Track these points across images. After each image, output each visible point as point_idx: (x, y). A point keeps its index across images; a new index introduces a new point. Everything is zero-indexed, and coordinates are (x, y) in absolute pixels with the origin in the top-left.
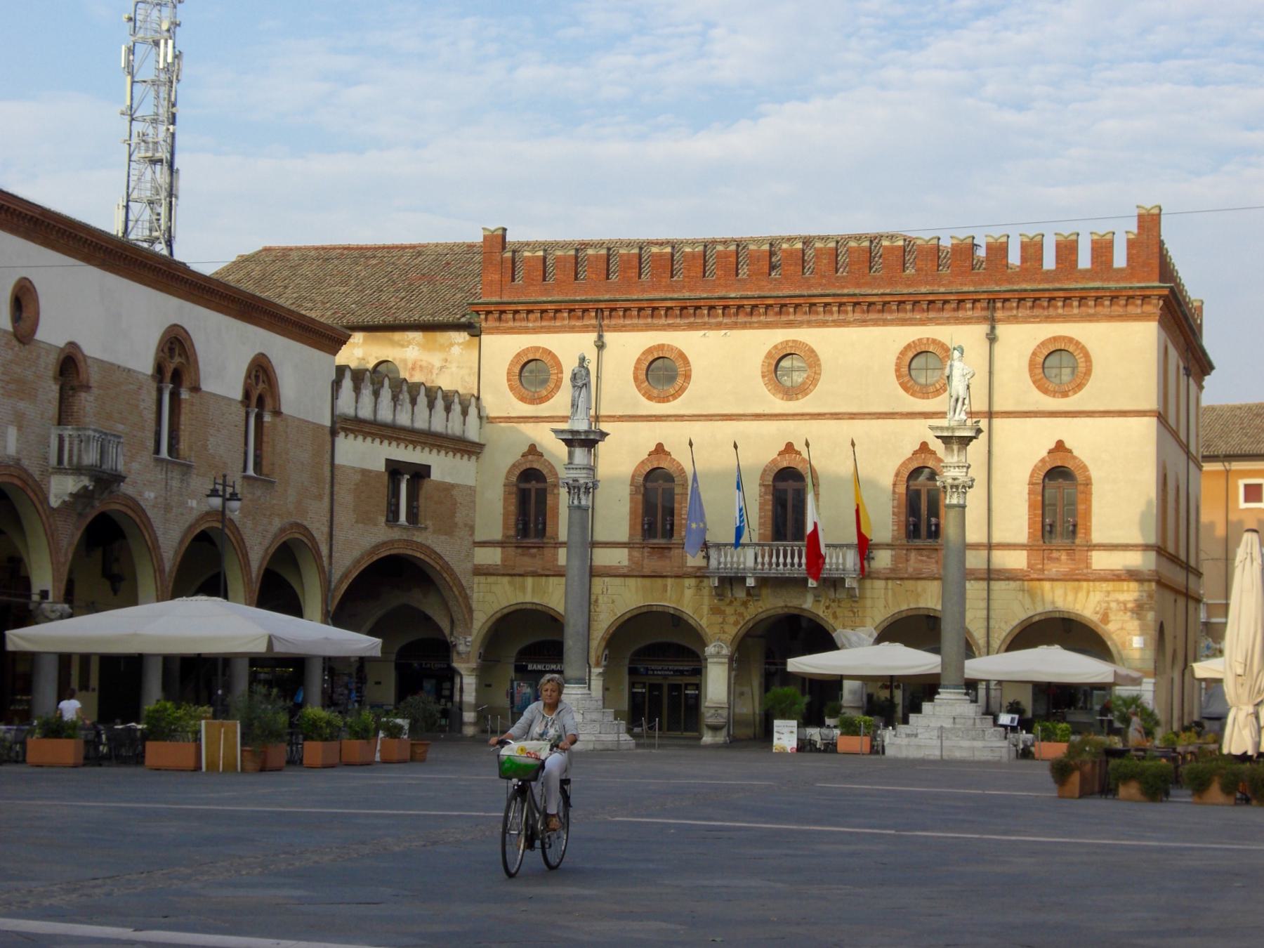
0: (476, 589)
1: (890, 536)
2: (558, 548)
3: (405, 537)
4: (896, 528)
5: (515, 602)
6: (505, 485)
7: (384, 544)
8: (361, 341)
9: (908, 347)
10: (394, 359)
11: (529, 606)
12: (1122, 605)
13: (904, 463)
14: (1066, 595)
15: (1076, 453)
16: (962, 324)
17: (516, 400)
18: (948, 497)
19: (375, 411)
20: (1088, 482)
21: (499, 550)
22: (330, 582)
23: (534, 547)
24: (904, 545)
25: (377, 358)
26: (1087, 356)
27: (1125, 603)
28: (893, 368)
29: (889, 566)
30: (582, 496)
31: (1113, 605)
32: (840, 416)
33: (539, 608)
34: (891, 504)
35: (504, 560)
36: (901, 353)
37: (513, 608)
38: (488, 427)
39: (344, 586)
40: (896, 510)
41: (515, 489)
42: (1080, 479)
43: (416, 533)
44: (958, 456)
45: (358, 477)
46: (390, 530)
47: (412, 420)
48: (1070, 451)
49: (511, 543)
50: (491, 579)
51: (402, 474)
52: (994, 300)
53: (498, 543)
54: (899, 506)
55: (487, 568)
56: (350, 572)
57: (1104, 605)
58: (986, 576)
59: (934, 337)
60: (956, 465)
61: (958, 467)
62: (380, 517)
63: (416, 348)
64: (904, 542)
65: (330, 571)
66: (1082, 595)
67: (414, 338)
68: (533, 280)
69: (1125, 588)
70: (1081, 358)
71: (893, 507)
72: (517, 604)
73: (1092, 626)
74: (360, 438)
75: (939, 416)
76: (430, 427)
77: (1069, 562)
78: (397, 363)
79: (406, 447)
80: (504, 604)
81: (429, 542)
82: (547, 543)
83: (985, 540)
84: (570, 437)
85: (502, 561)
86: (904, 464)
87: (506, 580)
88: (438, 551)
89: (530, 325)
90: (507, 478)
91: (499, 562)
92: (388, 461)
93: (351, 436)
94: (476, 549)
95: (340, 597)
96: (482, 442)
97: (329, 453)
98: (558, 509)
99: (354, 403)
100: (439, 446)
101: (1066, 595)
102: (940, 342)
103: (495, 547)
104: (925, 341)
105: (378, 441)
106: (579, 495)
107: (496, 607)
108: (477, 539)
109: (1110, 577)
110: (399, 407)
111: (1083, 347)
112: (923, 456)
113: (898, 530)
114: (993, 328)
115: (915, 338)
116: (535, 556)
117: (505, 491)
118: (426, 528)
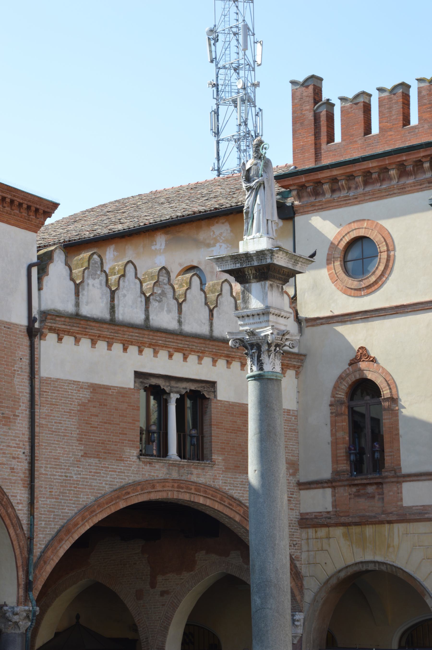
0: (305, 548)
2: (400, 483)
3: (175, 475)
5: (353, 562)
6: (331, 405)
7: (135, 485)
8: (163, 247)
10: (199, 263)
11: (371, 567)
17: (339, 293)
19: (112, 309)
21: (329, 491)
22: (31, 539)
23: (371, 484)
25: (180, 265)
30: (264, 357)
33: (383, 568)
35: (335, 505)
37: (351, 571)
38: (309, 331)
39: (66, 546)
41: (344, 409)
43: (195, 471)
45: (86, 394)
46: (148, 467)
47: (180, 322)
49: (342, 481)
50: (322, 532)
51: (169, 394)
53: (326, 482)
55: (316, 518)
56: (76, 524)
62: (127, 449)
63: (224, 246)
65: (31, 525)
67: (221, 234)
68: (352, 135)
72: (356, 564)
74: (85, 342)
76: (211, 330)
78: (202, 267)
79: (170, 356)
80: (340, 565)
81: (219, 483)
82: (386, 477)
84: (238, 266)
85: (333, 506)
87: (338, 532)
88: (236, 495)
89: (351, 194)
90: (333, 396)
91: (330, 509)
92: (138, 375)
93: (68, 340)
94: (302, 492)
95: (57, 560)
96: (303, 352)
97: (26, 361)
98: (398, 429)
99: (73, 297)
100: (227, 356)
103: (323, 488)
105: (117, 347)
106: (259, 356)
107: (331, 570)
108: (301, 481)
110: (154, 305)
116: (373, 497)
117: (331, 413)
118: (213, 464)
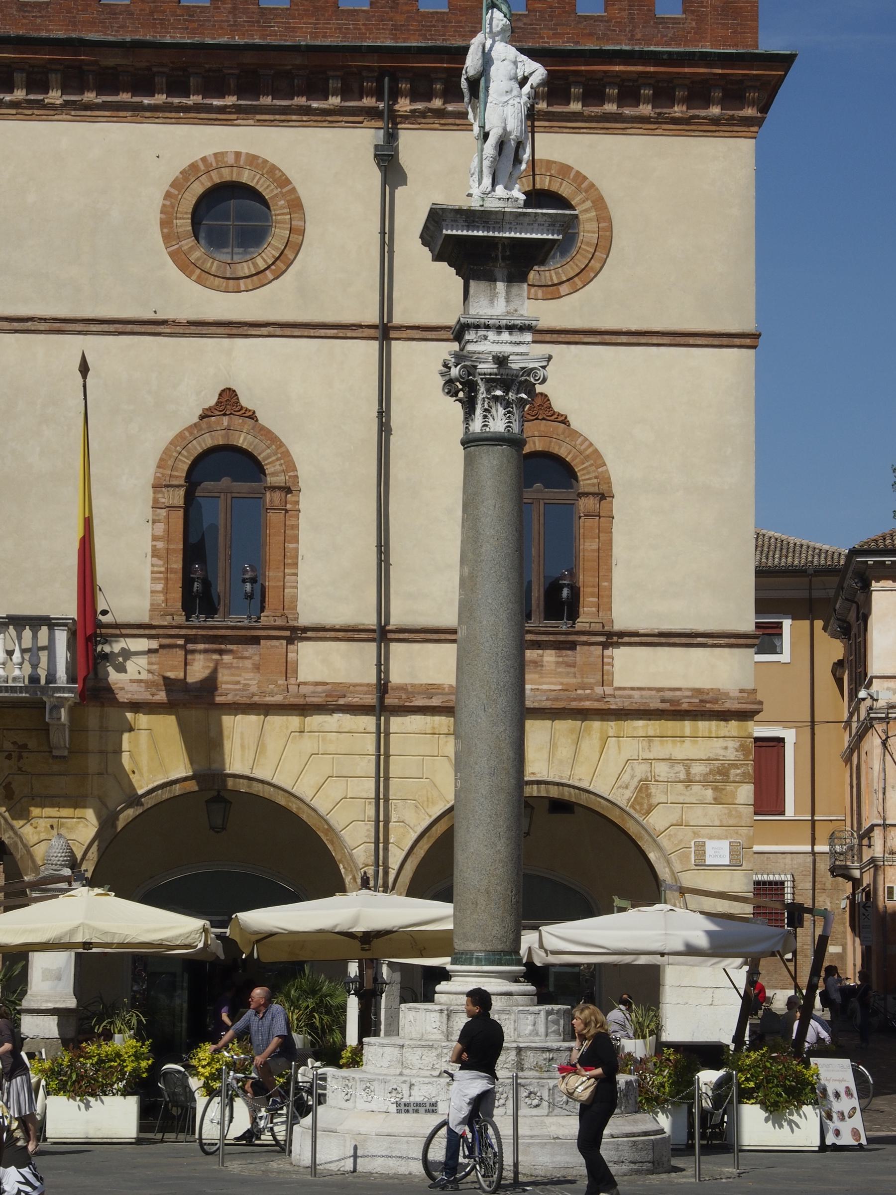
1: (148, 607)
4: (160, 587)
9: (192, 171)
12: (680, 768)
13: (180, 435)
14: (553, 746)
15: (575, 424)
16: (317, 124)
18: (479, 411)
20: (604, 488)
24: (179, 627)
26: (600, 204)
27: (687, 763)
28: (155, 217)
29: (145, 676)
31: (662, 770)
32: (28, 325)
34: (147, 532)
36: (174, 184)
40: (160, 545)
42: (586, 481)
44: (508, 300)
48: (564, 421)
52: (394, 81)
54: (168, 537)
57: (641, 770)
58: (371, 699)
59: (252, 152)
60: (504, 322)
61: (511, 328)
64: (180, 619)
66: (590, 745)
69: (687, 732)
70: (586, 211)
71: (155, 538)
73: (614, 816)
75: (264, 331)
77: (559, 670)
83: (370, 620)
86: (181, 440)
101: (553, 746)
102: (265, 161)
104: (231, 160)
109: (655, 704)
111: (592, 185)
112: (225, 421)
113: (166, 591)
114: (391, 137)
115: (209, 152)
